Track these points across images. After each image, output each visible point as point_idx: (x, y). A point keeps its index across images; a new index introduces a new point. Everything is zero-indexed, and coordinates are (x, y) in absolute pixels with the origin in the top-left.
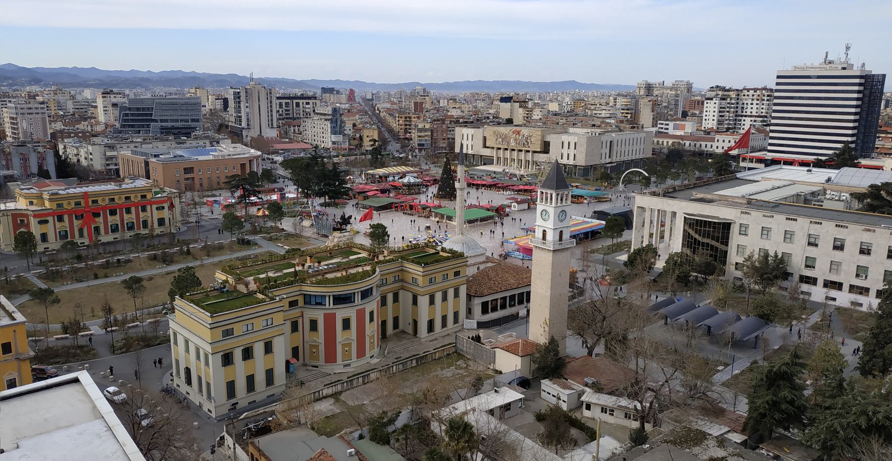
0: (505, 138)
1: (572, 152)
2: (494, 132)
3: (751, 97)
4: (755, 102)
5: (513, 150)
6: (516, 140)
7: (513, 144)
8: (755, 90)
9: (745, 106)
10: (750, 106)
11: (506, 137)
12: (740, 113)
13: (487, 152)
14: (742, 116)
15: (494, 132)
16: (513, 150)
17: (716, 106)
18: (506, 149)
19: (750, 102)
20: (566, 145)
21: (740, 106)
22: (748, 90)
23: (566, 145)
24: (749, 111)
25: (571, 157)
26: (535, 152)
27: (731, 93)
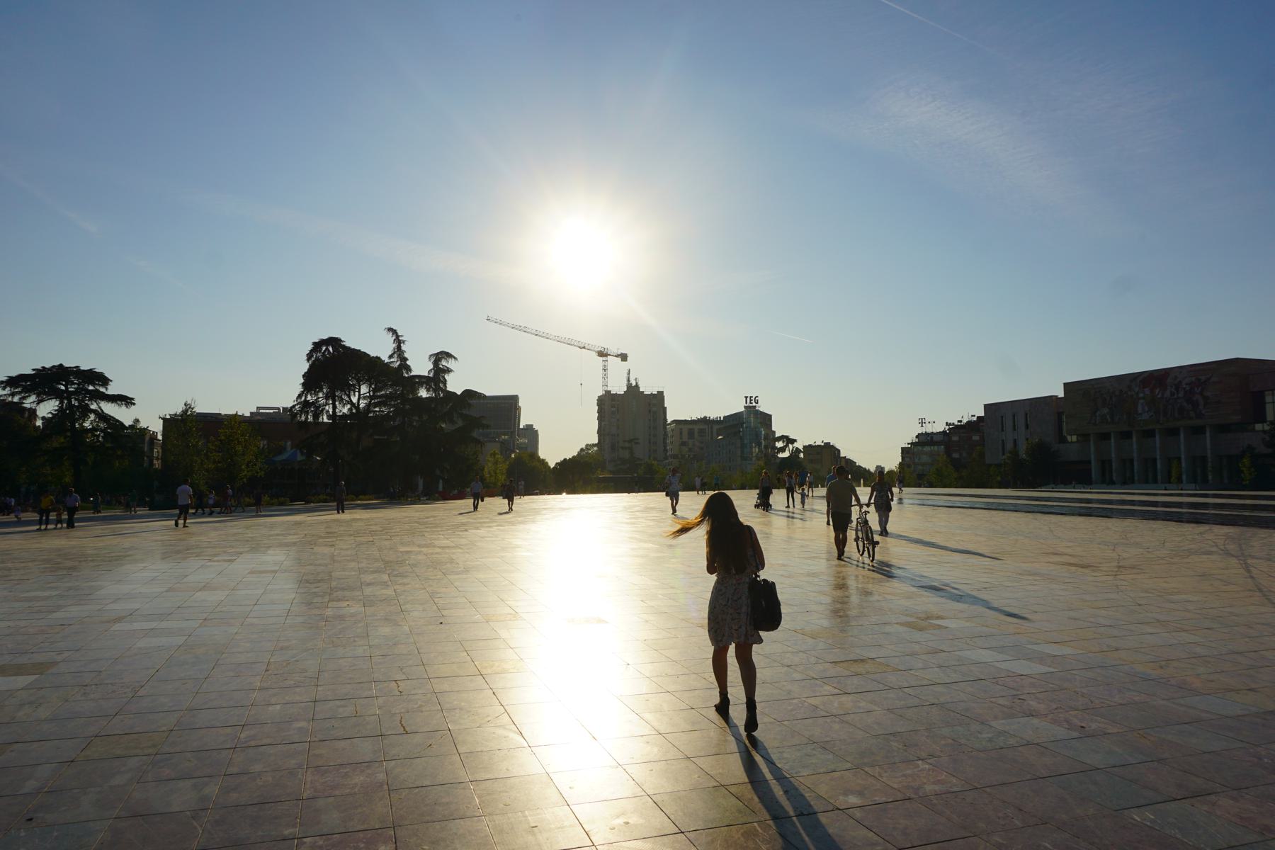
16: (1150, 434)
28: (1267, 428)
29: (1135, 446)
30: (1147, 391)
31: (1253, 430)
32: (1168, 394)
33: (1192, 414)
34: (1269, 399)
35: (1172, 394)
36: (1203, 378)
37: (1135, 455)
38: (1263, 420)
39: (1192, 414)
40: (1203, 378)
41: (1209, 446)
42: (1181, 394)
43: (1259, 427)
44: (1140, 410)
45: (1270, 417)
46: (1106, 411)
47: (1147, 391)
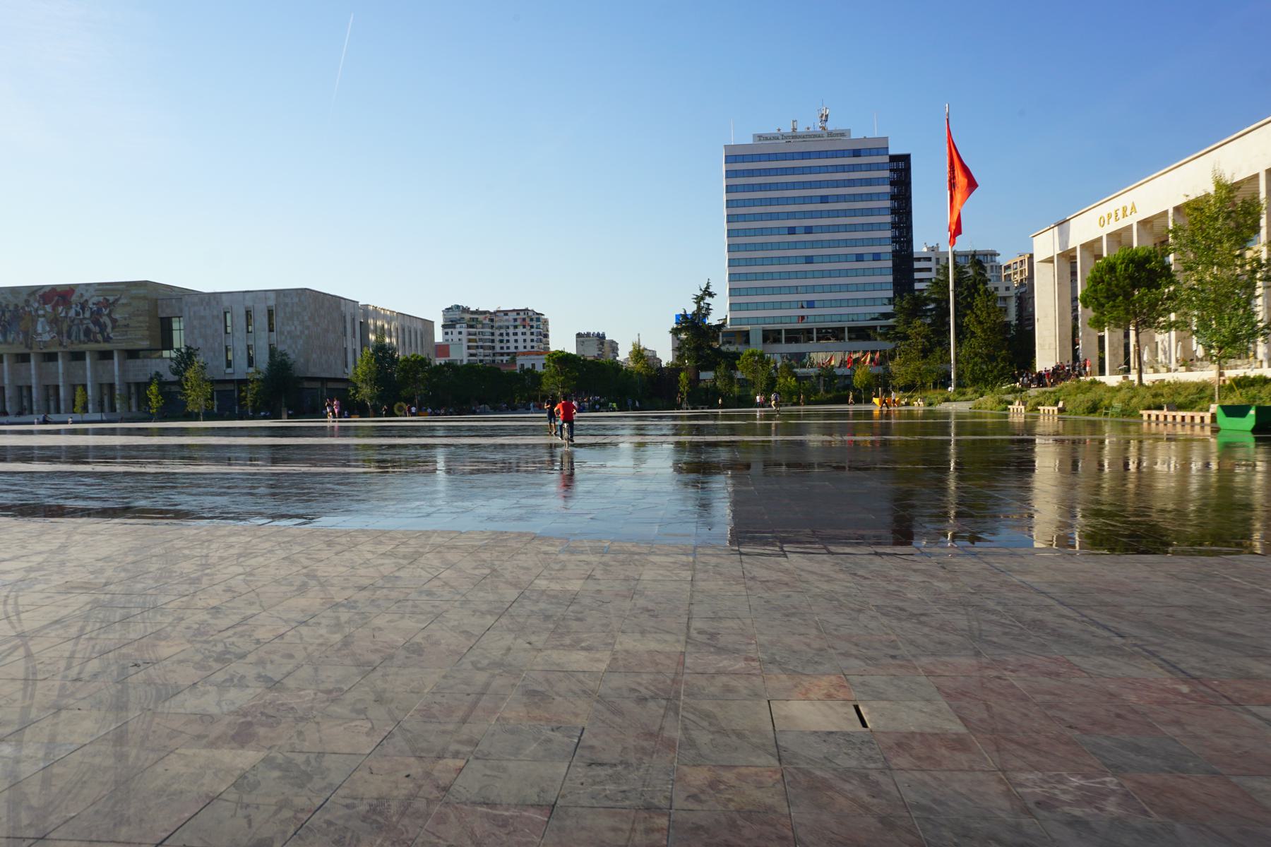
3: (512, 323)
4: (520, 330)
5: (52, 357)
6: (54, 321)
8: (518, 312)
9: (505, 338)
10: (512, 338)
12: (498, 350)
14: (502, 354)
16: (52, 357)
17: (464, 337)
18: (24, 358)
19: (511, 331)
21: (497, 338)
22: (506, 313)
24: (512, 345)
26: (132, 354)
27: (481, 317)
28: (174, 355)
29: (33, 372)
31: (161, 357)
32: (72, 313)
33: (99, 337)
34: (175, 325)
35: (77, 314)
36: (111, 299)
37: (34, 382)
38: (170, 348)
39: (99, 337)
40: (111, 299)
41: (116, 373)
42: (87, 314)
43: (166, 353)
44: (40, 330)
45: (176, 345)
47: (48, 308)
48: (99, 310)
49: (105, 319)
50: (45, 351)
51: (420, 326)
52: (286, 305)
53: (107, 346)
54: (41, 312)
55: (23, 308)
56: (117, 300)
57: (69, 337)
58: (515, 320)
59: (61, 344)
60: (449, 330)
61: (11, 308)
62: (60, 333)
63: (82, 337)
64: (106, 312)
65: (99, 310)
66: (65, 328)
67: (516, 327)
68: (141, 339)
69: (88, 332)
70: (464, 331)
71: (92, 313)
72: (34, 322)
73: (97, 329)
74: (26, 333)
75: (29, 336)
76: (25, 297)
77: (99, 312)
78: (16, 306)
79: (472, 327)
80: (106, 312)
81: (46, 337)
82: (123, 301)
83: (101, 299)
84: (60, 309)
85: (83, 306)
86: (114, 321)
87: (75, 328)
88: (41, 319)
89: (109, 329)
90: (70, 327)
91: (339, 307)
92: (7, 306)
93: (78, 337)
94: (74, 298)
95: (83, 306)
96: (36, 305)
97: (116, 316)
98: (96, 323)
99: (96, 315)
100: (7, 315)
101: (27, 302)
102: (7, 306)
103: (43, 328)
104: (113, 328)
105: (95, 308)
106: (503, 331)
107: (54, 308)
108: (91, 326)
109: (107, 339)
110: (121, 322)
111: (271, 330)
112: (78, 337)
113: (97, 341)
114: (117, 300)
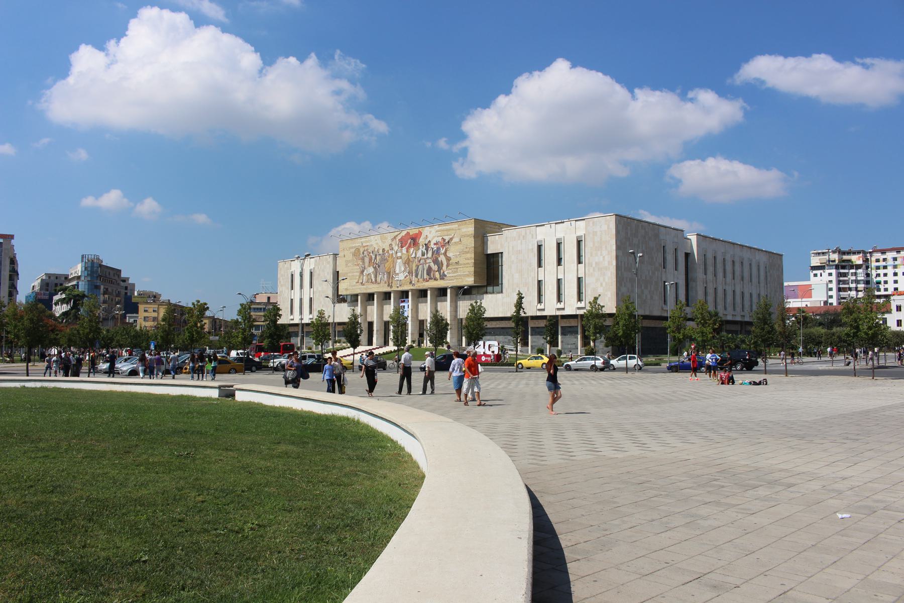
0: (379, 262)
1: (570, 272)
2: (356, 253)
3: (890, 262)
5: (404, 295)
6: (408, 262)
7: (402, 279)
10: (890, 278)
11: (384, 260)
13: (342, 314)
15: (356, 253)
17: (834, 278)
18: (387, 296)
19: (890, 271)
20: (550, 255)
23: (550, 255)
25: (570, 290)
30: (404, 249)
32: (419, 254)
33: (437, 275)
35: (423, 255)
40: (447, 239)
42: (430, 255)
46: (371, 270)
47: (404, 249)
48: (438, 249)
49: (442, 258)
50: (400, 289)
51: (763, 259)
52: (595, 233)
53: (441, 284)
54: (399, 254)
55: (388, 252)
56: (451, 239)
57: (416, 276)
58: (895, 259)
59: (411, 283)
60: (818, 272)
61: (381, 252)
62: (410, 273)
63: (426, 276)
64: (442, 251)
65: (438, 249)
66: (414, 268)
67: (895, 267)
68: (468, 276)
69: (430, 270)
70: (834, 271)
71: (433, 253)
72: (394, 263)
73: (435, 267)
74: (389, 273)
75: (390, 275)
76: (390, 242)
77: (437, 252)
78: (383, 250)
79: (843, 267)
80: (442, 251)
81: (401, 277)
82: (456, 240)
83: (440, 239)
84: (412, 250)
85: (427, 246)
86: (448, 259)
87: (420, 267)
88: (399, 261)
89: (444, 268)
90: (418, 267)
91: (657, 236)
92: (378, 251)
93: (422, 276)
94: (421, 241)
95: (427, 246)
96: (396, 248)
97: (449, 254)
98: (436, 261)
99: (437, 252)
100: (378, 258)
101: (391, 245)
102: (378, 251)
103: (400, 268)
104: (447, 266)
105: (435, 248)
106: (882, 272)
107: (407, 251)
108: (432, 265)
109: (443, 277)
110: (453, 261)
111: (579, 262)
112: (422, 276)
113: (436, 279)
114: (451, 239)
